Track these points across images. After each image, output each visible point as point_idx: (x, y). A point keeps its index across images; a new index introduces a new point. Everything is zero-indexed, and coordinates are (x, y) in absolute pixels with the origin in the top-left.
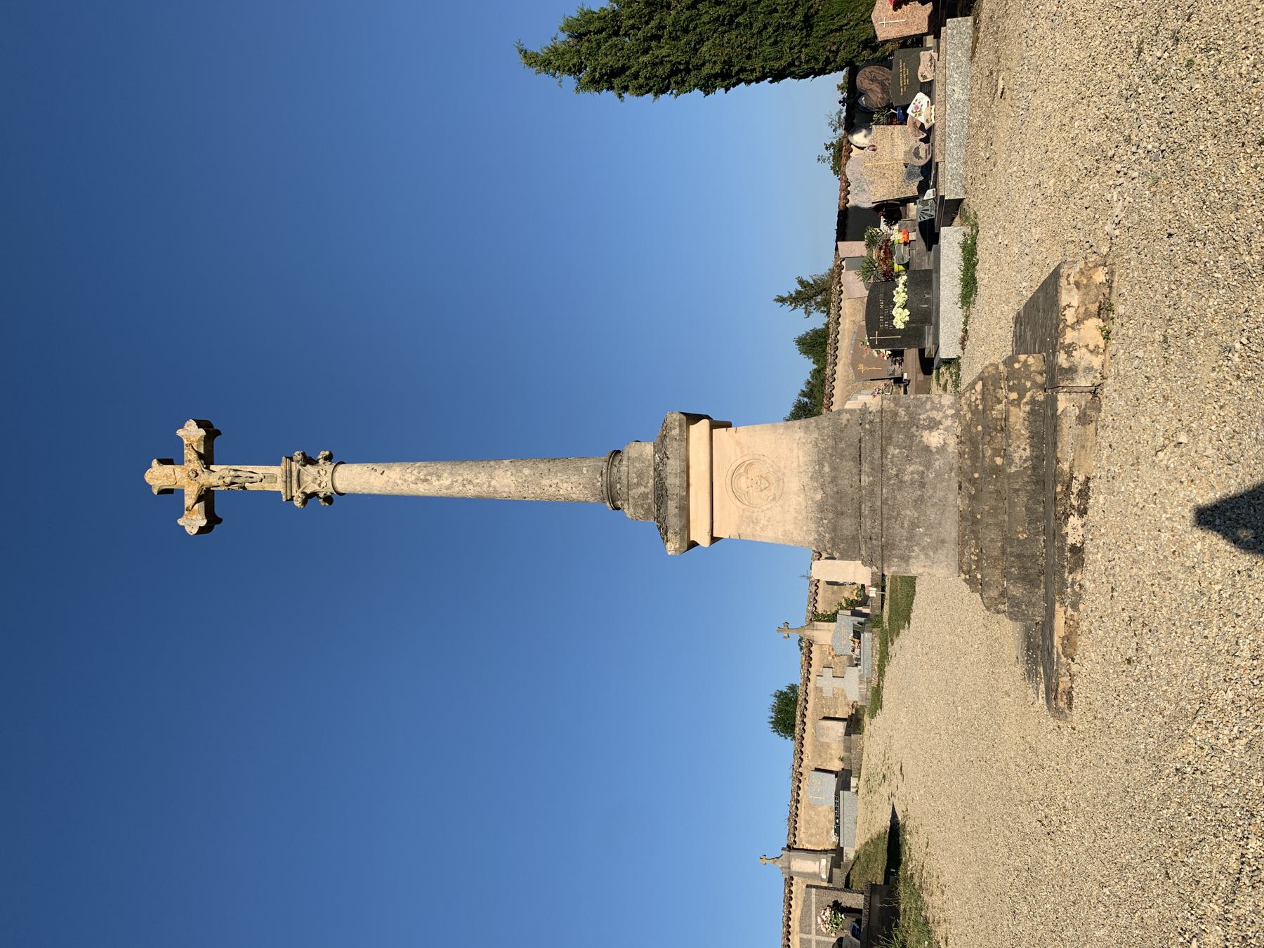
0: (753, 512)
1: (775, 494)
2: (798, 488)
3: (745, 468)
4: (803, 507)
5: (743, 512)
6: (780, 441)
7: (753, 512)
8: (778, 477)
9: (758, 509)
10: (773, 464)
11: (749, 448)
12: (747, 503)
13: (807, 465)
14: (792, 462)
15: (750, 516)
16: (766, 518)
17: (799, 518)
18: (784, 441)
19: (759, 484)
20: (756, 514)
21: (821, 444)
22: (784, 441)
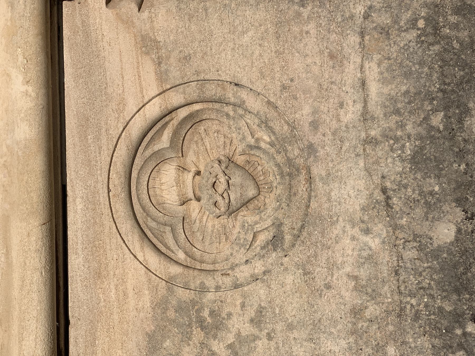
0: (203, 289)
1: (278, 225)
2: (363, 201)
3: (176, 133)
4: (385, 271)
5: (170, 290)
6: (296, 29)
7: (203, 289)
8: (289, 162)
9: (220, 279)
10: (272, 114)
11: (187, 58)
12: (181, 256)
13: (397, 112)
14: (341, 105)
15: (193, 303)
16: (250, 313)
17: (368, 314)
18: (311, 27)
19: (221, 187)
20: (210, 296)
21: (456, 26)
22: (311, 27)
